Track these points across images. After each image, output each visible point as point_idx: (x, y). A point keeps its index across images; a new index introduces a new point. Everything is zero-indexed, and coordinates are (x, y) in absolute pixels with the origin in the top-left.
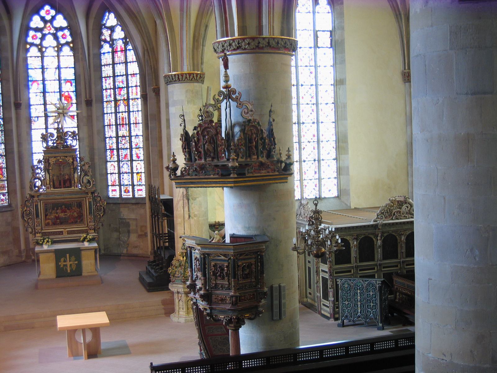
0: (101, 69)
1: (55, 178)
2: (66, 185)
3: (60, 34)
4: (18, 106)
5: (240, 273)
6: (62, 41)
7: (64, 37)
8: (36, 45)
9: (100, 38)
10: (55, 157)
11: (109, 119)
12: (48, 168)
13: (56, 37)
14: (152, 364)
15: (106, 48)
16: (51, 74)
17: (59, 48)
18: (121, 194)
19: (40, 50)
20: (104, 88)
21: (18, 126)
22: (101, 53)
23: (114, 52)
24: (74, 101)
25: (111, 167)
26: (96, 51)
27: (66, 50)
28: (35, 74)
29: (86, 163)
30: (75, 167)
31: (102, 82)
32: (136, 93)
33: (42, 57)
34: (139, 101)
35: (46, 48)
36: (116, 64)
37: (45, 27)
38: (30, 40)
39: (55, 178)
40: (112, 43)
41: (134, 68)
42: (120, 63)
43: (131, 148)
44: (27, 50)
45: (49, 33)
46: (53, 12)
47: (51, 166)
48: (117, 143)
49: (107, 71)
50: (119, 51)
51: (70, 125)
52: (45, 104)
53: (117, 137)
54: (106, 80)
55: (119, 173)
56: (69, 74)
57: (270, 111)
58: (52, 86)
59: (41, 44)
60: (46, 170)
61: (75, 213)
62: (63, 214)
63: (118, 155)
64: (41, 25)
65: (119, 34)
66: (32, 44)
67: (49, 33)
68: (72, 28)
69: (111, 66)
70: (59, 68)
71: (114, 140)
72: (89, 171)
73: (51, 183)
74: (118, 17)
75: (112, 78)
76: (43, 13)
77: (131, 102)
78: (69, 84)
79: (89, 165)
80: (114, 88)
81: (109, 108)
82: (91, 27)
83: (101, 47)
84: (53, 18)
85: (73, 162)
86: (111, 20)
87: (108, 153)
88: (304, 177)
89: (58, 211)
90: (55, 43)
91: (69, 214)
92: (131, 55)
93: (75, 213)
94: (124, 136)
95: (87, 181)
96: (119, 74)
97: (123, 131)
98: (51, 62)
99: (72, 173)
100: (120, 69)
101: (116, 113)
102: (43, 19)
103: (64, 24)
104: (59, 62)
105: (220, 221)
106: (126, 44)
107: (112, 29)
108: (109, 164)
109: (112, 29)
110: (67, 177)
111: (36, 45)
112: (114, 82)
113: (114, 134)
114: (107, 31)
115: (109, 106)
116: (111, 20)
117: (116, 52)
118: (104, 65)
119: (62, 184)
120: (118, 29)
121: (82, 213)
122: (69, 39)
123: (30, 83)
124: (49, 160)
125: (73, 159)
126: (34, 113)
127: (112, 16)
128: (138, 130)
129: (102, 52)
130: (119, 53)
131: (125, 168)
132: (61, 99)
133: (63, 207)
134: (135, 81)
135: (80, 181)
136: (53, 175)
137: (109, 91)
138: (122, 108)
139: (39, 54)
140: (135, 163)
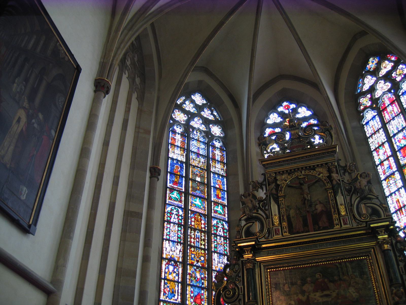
0: (368, 142)
1: (292, 213)
2: (320, 224)
9: (357, 110)
10: (290, 172)
12: (274, 191)
20: (377, 162)
22: (363, 125)
26: (355, 124)
29: (361, 176)
30: (334, 183)
31: (372, 157)
36: (387, 123)
39: (292, 212)
42: (393, 119)
46: (293, 106)
47: (281, 191)
50: (388, 106)
54: (377, 152)
61: (352, 290)
62: (318, 294)
69: (381, 131)
72: (370, 190)
73: (285, 224)
75: (387, 145)
76: (280, 109)
79: (367, 179)
82: (342, 101)
85: (330, 177)
89: (305, 288)
91: (334, 294)
93: (352, 290)
95: (370, 210)
96: (396, 131)
99: (331, 196)
102: (281, 114)
103: (308, 113)
107: (372, 89)
109: (372, 89)
110: (319, 208)
114: (366, 97)
115: (391, 182)
117: (385, 109)
118: (370, 136)
119: (310, 221)
121: (370, 289)
124: (276, 180)
125: (330, 171)
129: (364, 123)
133: (317, 276)
135: (351, 211)
136: (288, 206)
137: (386, 163)
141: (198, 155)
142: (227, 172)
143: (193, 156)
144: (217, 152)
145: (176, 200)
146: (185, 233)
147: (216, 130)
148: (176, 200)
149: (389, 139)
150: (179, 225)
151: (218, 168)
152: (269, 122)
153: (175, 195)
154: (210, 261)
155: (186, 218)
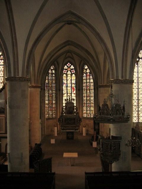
3: (72, 71)
4: (59, 90)
5: (112, 148)
6: (73, 73)
7: (73, 71)
8: (65, 74)
11: (85, 95)
13: (71, 72)
14: (85, 172)
15: (85, 75)
16: (69, 82)
17: (72, 75)
18: (87, 116)
19: (66, 75)
21: (59, 96)
23: (87, 76)
24: (75, 89)
25: (85, 108)
27: (74, 75)
28: (65, 81)
32: (92, 87)
33: (67, 77)
34: (93, 90)
35: (68, 74)
37: (68, 69)
38: (64, 72)
40: (86, 73)
41: (92, 81)
43: (90, 103)
44: (63, 75)
45: (69, 70)
48: (86, 102)
49: (85, 81)
51: (74, 96)
52: (67, 90)
53: (86, 100)
55: (87, 110)
56: (74, 82)
57: (124, 101)
58: (69, 85)
59: (67, 73)
60: (66, 109)
63: (86, 105)
64: (67, 68)
65: (88, 71)
66: (64, 73)
67: (69, 70)
68: (75, 69)
70: (71, 80)
71: (86, 101)
74: (88, 66)
76: (67, 65)
77: (91, 90)
78: (74, 85)
80: (86, 86)
81: (84, 92)
82: (80, 69)
83: (83, 74)
84: (70, 66)
86: (86, 67)
87: (84, 104)
88: (139, 116)
90: (70, 73)
92: (91, 77)
94: (88, 100)
97: (88, 98)
98: (69, 78)
100: (88, 81)
101: (87, 93)
102: (67, 66)
103: (73, 68)
104: (71, 78)
105: (56, 173)
106: (90, 74)
107: (86, 69)
108: (84, 107)
109: (86, 69)
111: (65, 74)
112: (86, 84)
113: (86, 99)
116: (86, 67)
120: (88, 69)
122: (74, 72)
123: (63, 84)
126: (64, 92)
127: (86, 66)
128: (92, 98)
130: (88, 76)
131: (88, 109)
132: (71, 89)
134: (92, 84)
138: (88, 92)
139: (66, 76)
140: (91, 108)
141: (50, 80)
142: (55, 82)
143: (49, 80)
144: (54, 78)
145: (47, 92)
146: (49, 99)
147: (54, 72)
148: (47, 92)
149: (86, 83)
150: (48, 97)
151: (54, 82)
152: (65, 68)
153: (47, 91)
154: (52, 102)
155: (49, 95)
